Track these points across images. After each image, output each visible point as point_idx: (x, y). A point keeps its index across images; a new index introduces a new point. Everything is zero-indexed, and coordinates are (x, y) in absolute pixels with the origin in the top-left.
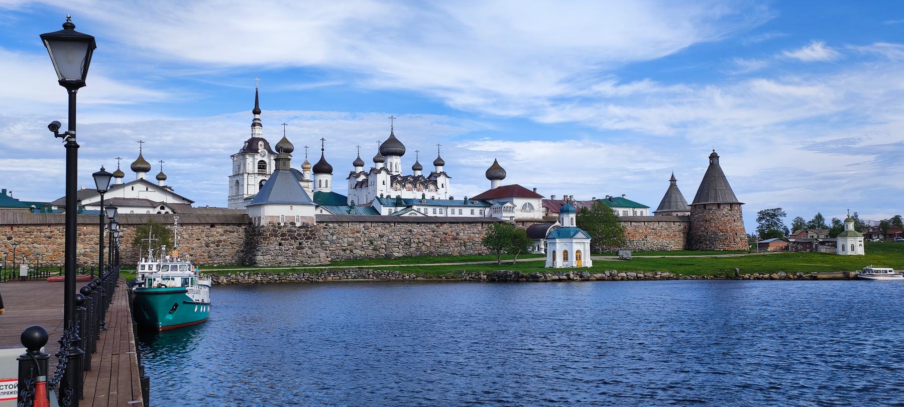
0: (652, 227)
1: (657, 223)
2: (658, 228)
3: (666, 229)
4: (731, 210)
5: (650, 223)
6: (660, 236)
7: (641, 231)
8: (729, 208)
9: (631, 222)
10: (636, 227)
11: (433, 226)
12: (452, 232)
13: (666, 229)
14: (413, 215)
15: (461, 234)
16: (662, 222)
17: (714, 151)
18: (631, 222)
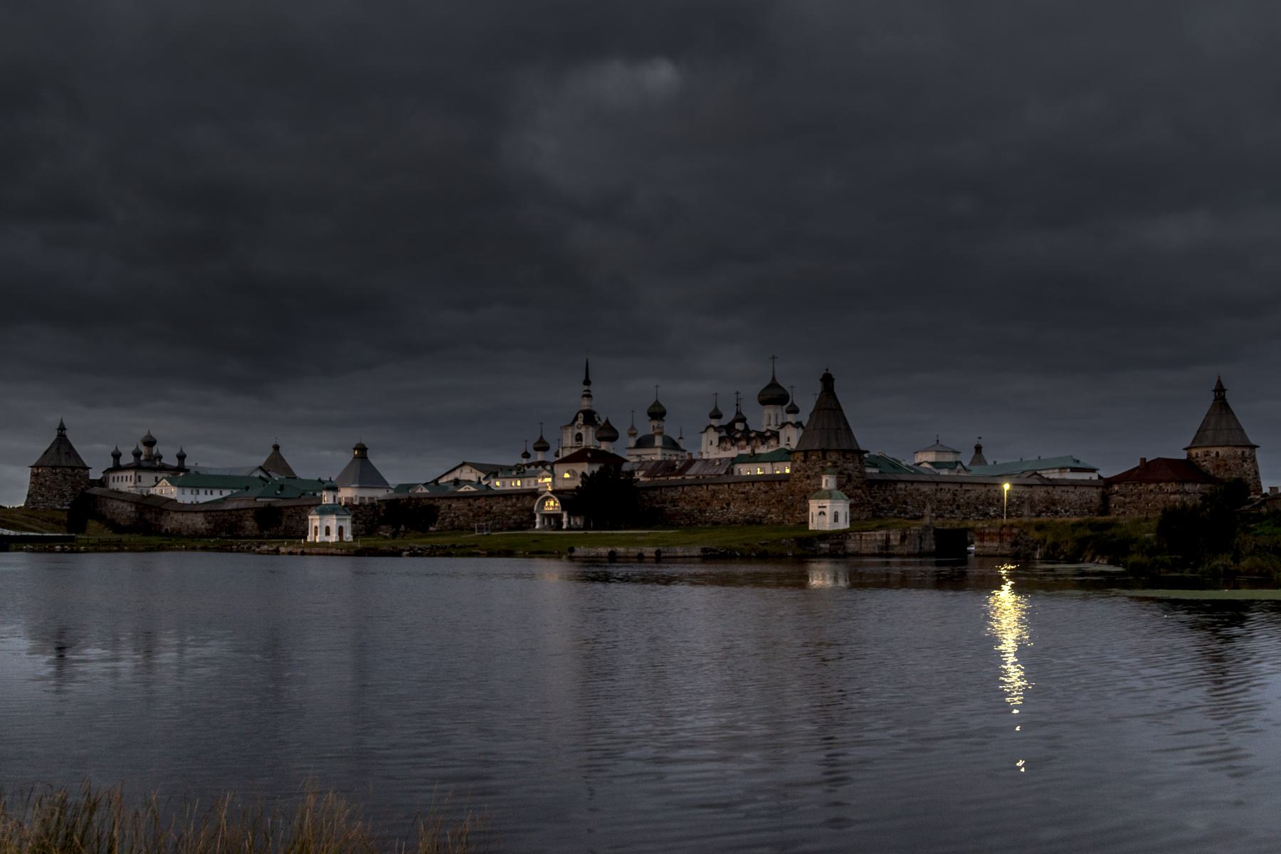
0: (740, 490)
1: (751, 484)
2: (753, 492)
3: (766, 492)
4: (804, 461)
5: (738, 485)
6: (753, 502)
7: (721, 497)
8: (802, 458)
9: (707, 485)
10: (714, 490)
11: (471, 500)
12: (486, 505)
13: (766, 492)
14: (467, 490)
15: (494, 508)
16: (759, 482)
17: (827, 370)
18: (707, 485)
